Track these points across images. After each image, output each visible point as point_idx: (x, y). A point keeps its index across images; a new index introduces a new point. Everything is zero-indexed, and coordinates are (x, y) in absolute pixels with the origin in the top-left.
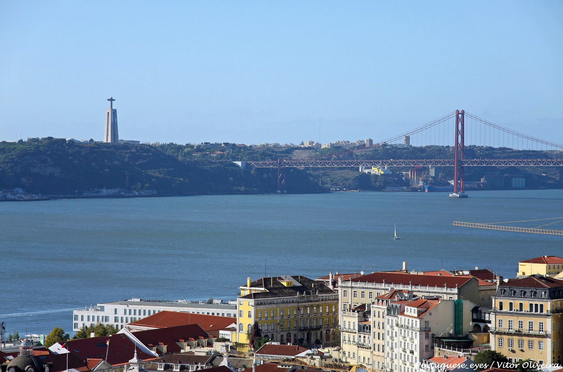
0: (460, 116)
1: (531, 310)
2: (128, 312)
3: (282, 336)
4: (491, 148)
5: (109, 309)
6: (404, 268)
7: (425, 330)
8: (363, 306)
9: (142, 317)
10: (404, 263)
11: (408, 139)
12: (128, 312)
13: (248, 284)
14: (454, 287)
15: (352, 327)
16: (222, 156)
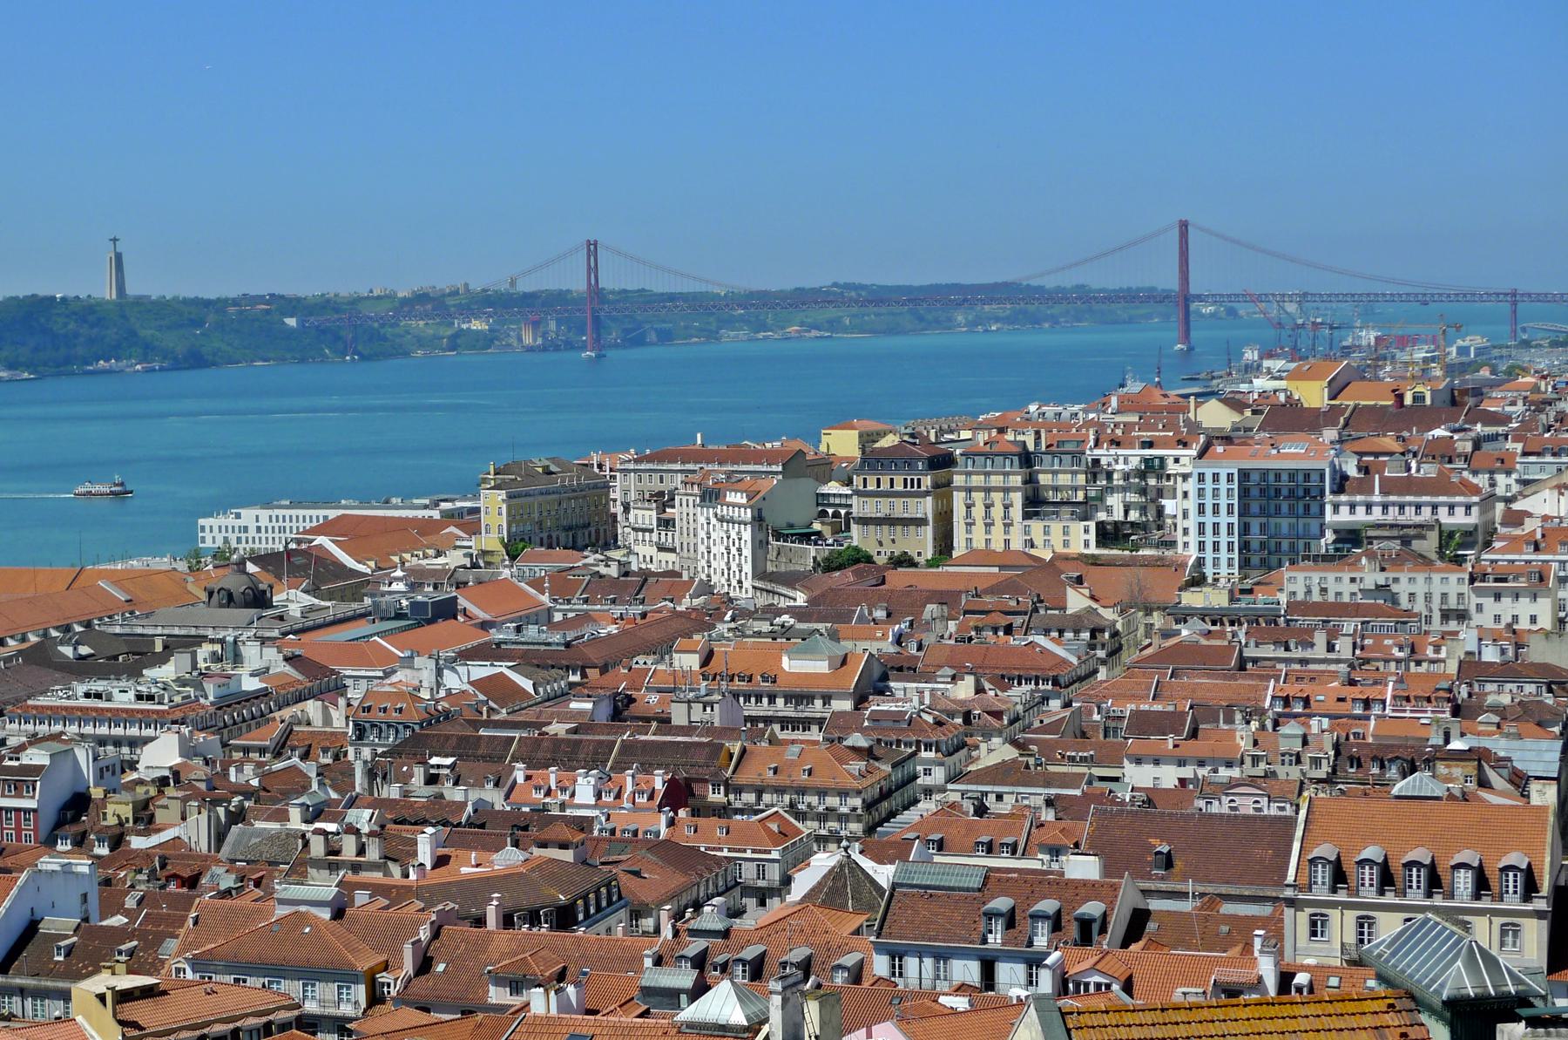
0: (592, 247)
1: (905, 486)
2: (274, 519)
3: (542, 539)
4: (625, 291)
5: (248, 516)
6: (699, 442)
7: (758, 520)
8: (661, 494)
9: (315, 524)
10: (699, 435)
11: (513, 283)
12: (274, 519)
13: (492, 472)
14: (777, 465)
15: (647, 522)
16: (267, 312)
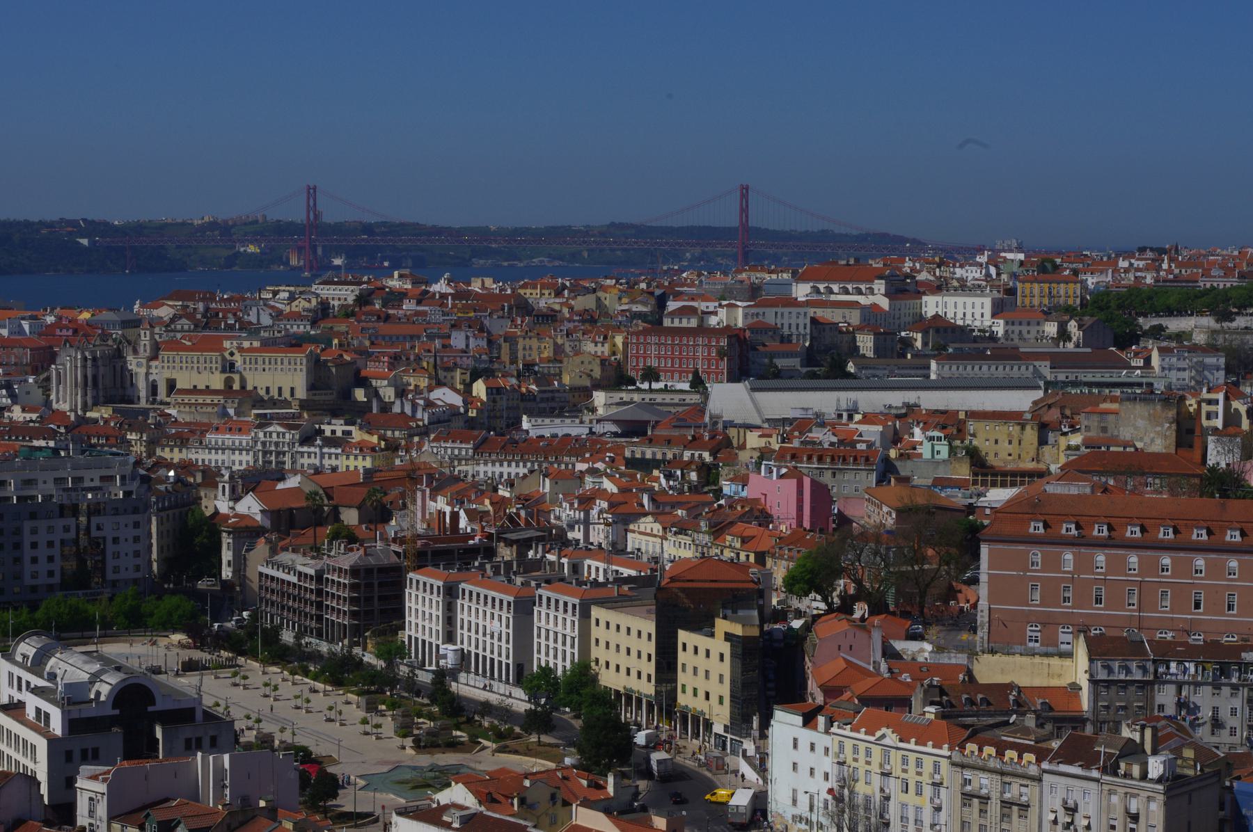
0: (312, 191)
